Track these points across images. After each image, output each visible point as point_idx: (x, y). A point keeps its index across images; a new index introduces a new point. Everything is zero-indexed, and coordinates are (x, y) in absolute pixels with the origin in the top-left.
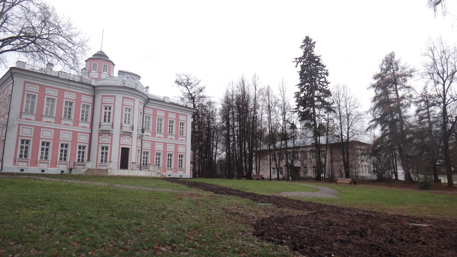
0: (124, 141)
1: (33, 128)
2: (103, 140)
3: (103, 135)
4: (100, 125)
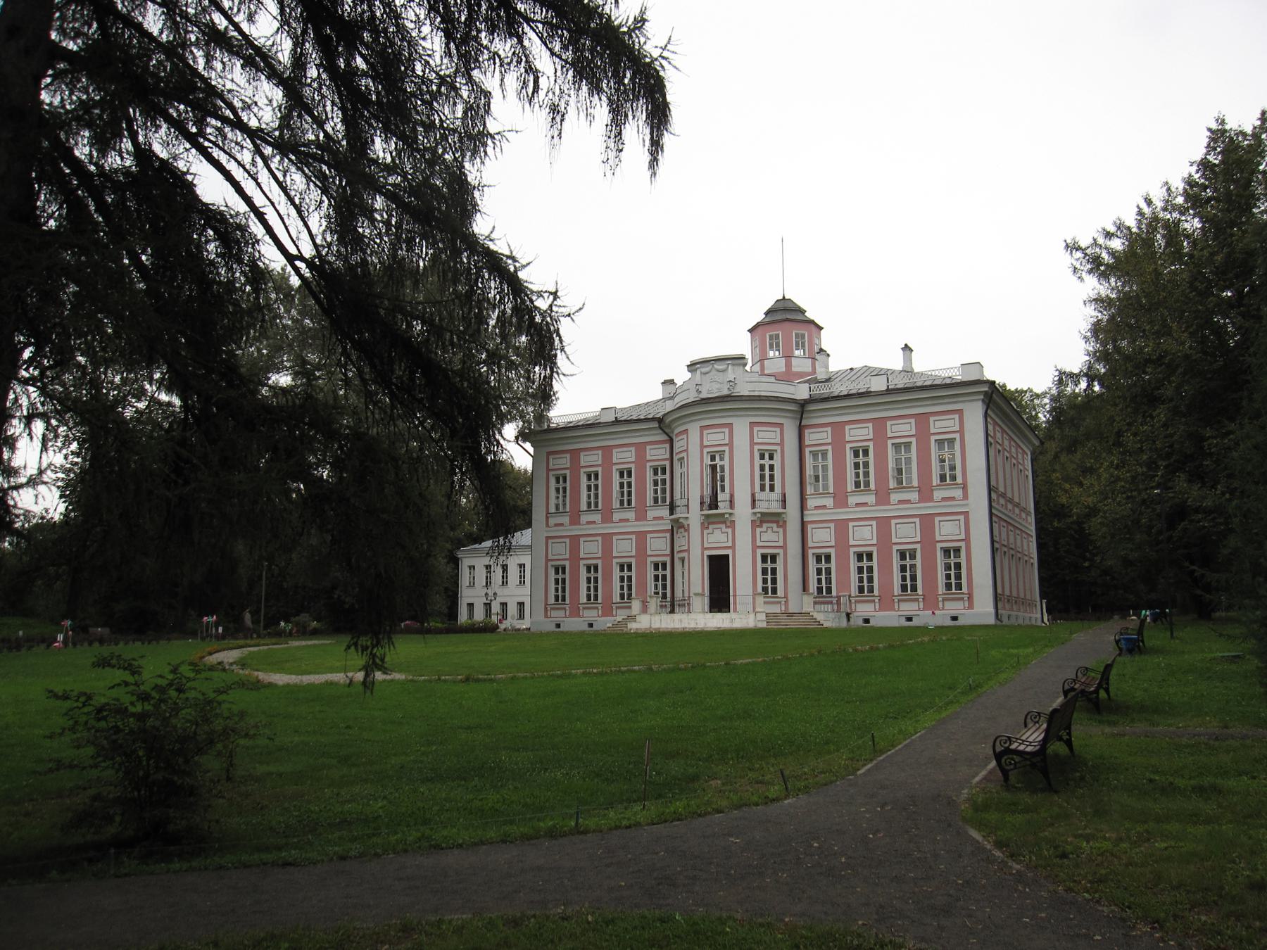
0: (712, 538)
1: (917, 520)
2: (765, 537)
3: (765, 525)
4: (754, 501)
